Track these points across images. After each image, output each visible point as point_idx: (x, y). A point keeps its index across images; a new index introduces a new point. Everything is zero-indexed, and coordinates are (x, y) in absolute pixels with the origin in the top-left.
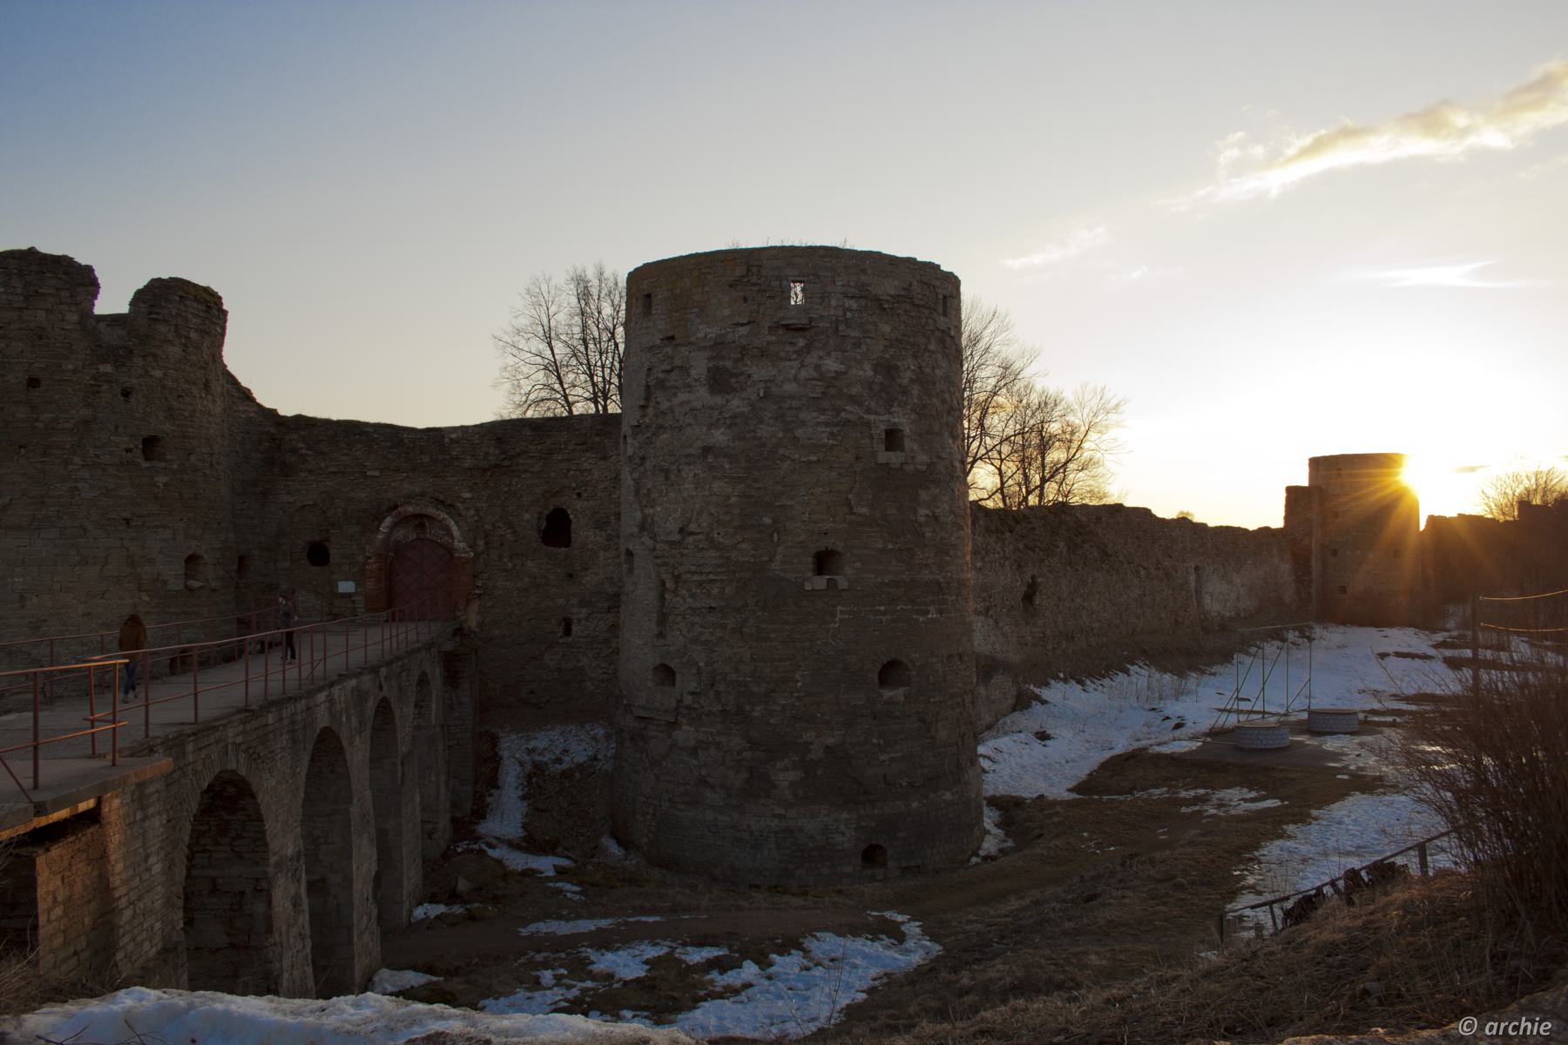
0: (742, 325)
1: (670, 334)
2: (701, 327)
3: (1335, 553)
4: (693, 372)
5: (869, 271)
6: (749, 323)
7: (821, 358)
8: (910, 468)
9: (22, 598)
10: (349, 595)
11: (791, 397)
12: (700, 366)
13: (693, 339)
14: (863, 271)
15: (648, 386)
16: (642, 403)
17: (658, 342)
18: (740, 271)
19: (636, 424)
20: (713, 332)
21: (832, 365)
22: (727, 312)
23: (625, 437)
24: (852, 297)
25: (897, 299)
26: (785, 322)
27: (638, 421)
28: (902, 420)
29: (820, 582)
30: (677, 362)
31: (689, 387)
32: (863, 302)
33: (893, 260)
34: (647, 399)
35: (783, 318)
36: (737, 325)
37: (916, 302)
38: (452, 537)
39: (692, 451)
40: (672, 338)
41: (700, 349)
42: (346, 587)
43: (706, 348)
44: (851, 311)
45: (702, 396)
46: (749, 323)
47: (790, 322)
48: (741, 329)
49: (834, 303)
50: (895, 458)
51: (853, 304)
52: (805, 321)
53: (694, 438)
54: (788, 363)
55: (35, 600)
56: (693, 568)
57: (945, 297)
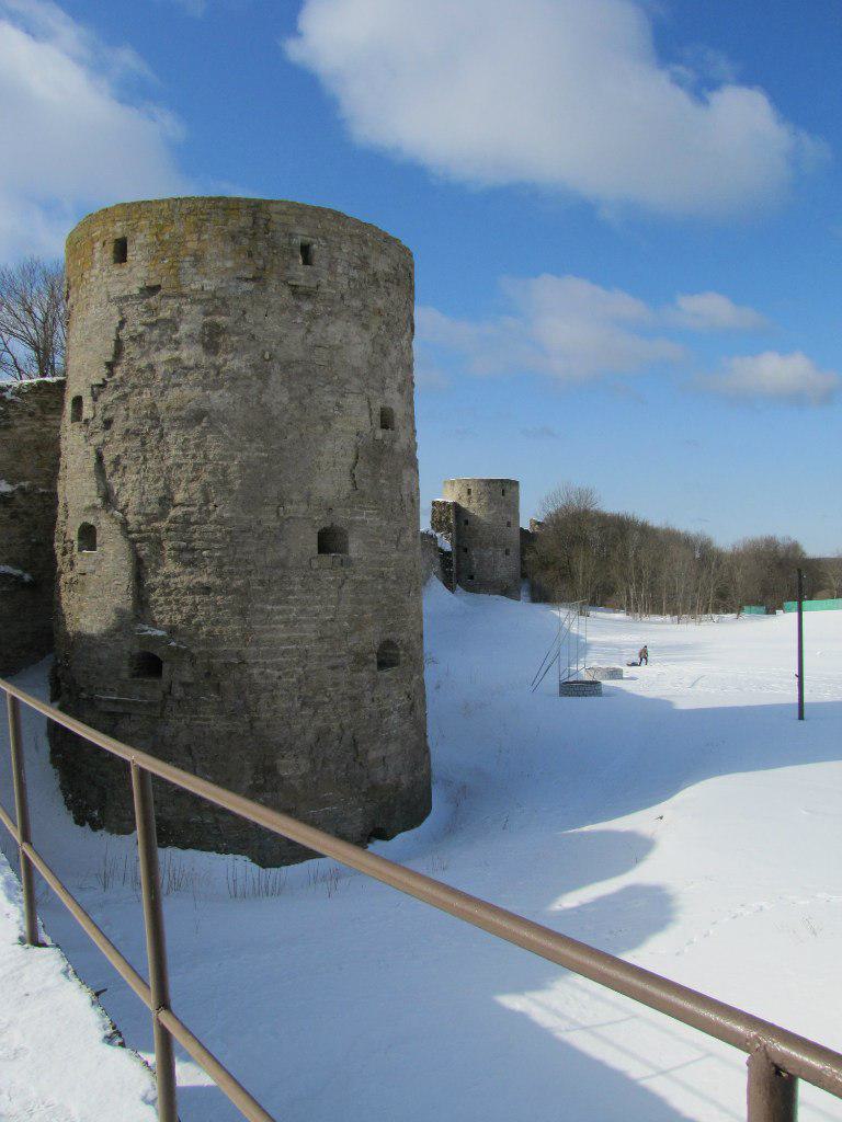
0: (247, 280)
1: (154, 283)
2: (196, 278)
3: (466, 550)
4: (184, 328)
6: (254, 279)
13: (186, 290)
15: (118, 343)
16: (109, 358)
19: (101, 382)
23: (78, 401)
27: (104, 379)
35: (292, 278)
40: (158, 288)
41: (194, 302)
45: (190, 354)
47: (298, 283)
49: (340, 270)
51: (354, 274)
53: (187, 399)
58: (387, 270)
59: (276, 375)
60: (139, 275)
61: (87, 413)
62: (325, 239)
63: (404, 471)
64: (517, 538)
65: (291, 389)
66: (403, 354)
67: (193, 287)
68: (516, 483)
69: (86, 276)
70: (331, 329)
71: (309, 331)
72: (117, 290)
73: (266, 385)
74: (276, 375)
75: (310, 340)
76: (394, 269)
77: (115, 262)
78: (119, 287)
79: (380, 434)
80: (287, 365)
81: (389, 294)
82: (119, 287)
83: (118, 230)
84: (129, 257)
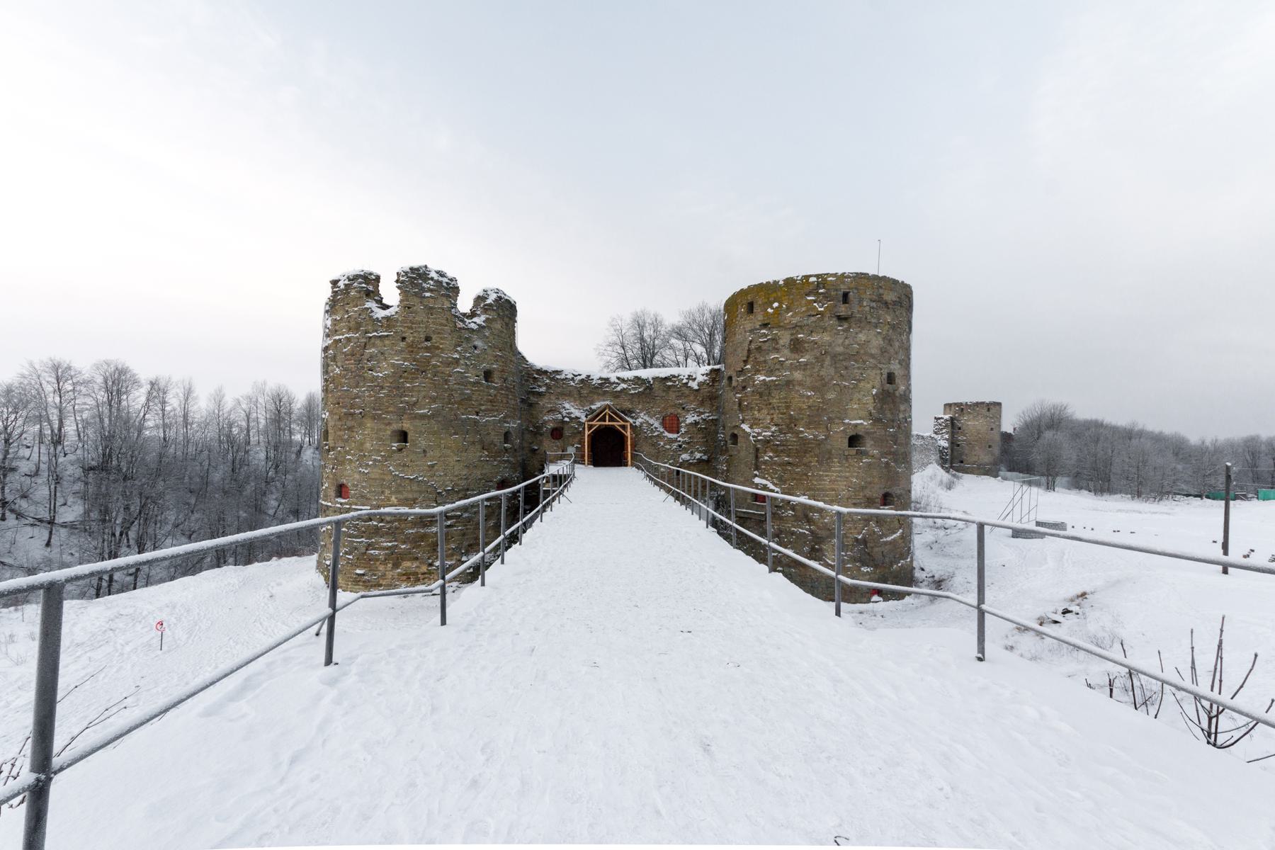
1: (766, 322)
4: (781, 342)
11: (840, 354)
12: (785, 338)
13: (782, 324)
14: (881, 287)
15: (749, 350)
16: (745, 359)
17: (758, 327)
22: (804, 309)
24: (874, 301)
25: (895, 303)
31: (777, 350)
32: (879, 304)
34: (748, 357)
36: (810, 316)
41: (786, 329)
44: (873, 308)
48: (813, 318)
49: (865, 304)
51: (874, 304)
52: (850, 313)
55: (432, 453)
58: (894, 299)
59: (828, 361)
60: (759, 319)
61: (734, 383)
62: (856, 289)
63: (901, 406)
64: (997, 438)
65: (835, 368)
66: (903, 343)
67: (785, 322)
68: (999, 404)
69: (734, 321)
70: (860, 335)
71: (846, 338)
72: (749, 326)
73: (822, 366)
74: (828, 361)
76: (899, 297)
77: (748, 313)
78: (750, 325)
81: (895, 312)
83: (750, 298)
84: (755, 311)
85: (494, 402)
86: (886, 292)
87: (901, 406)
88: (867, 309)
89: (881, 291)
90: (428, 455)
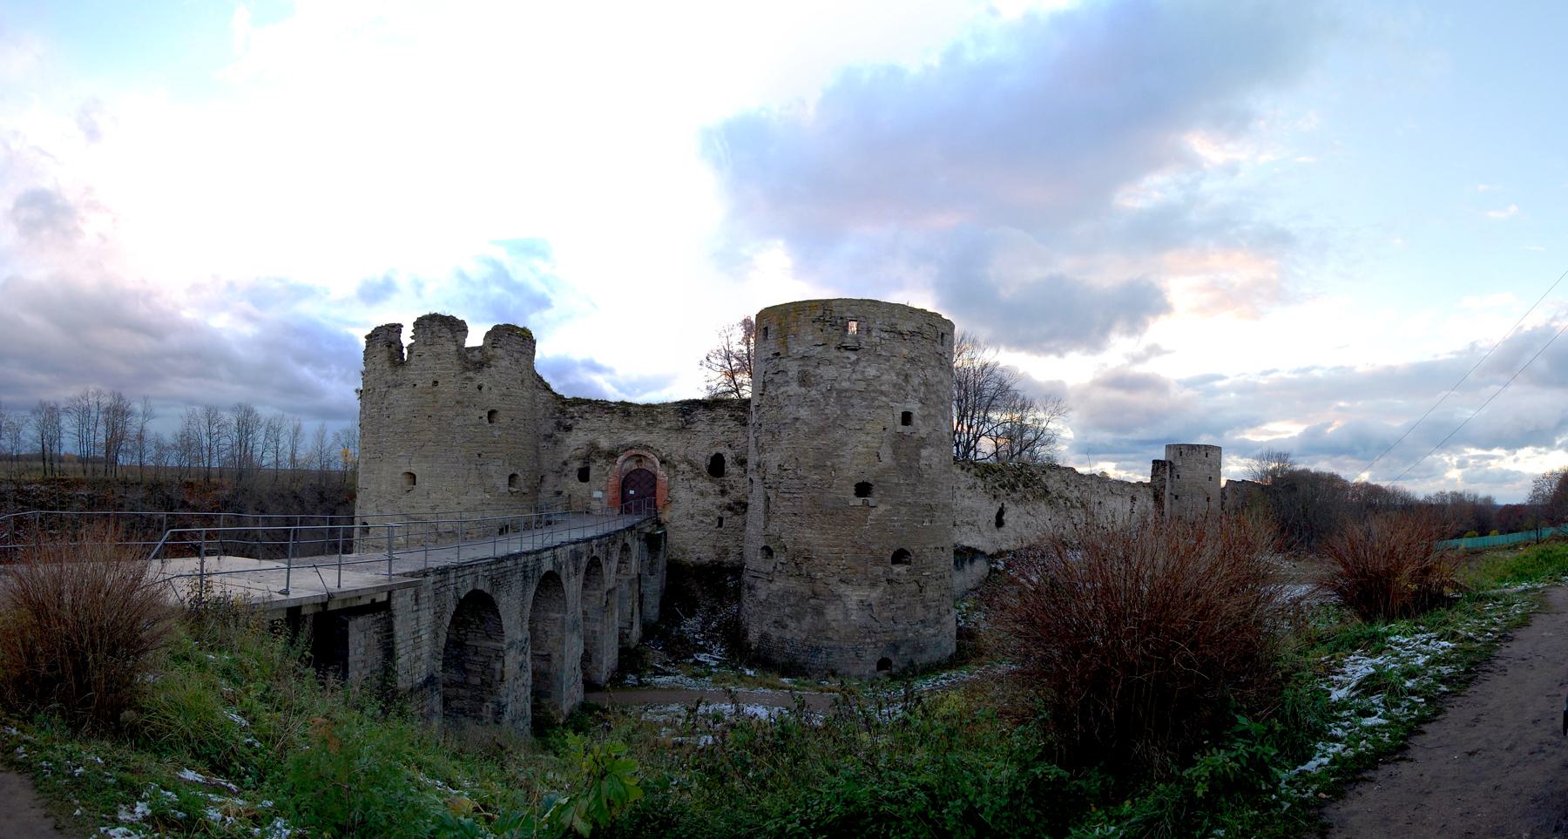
3: (1177, 497)
4: (790, 373)
5: (897, 316)
6: (823, 345)
7: (865, 367)
8: (916, 436)
9: (428, 493)
10: (599, 499)
11: (846, 391)
12: (793, 368)
13: (790, 354)
14: (894, 316)
16: (761, 392)
17: (771, 356)
18: (819, 313)
20: (802, 350)
21: (871, 372)
22: (810, 338)
26: (844, 345)
28: (914, 407)
29: (859, 501)
30: (781, 368)
32: (892, 335)
33: (913, 310)
34: (764, 390)
37: (925, 336)
38: (655, 467)
39: (787, 421)
40: (778, 354)
42: (597, 494)
43: (796, 359)
45: (794, 388)
46: (823, 345)
48: (818, 348)
49: (874, 334)
50: (907, 430)
51: (886, 335)
54: (845, 370)
56: (786, 490)
57: (943, 334)
75: (854, 376)
78: (764, 353)
79: (900, 428)
80: (840, 392)
82: (764, 353)
85: (498, 443)
86: (900, 322)
87: (922, 450)
88: (878, 340)
89: (894, 320)
90: (431, 497)
